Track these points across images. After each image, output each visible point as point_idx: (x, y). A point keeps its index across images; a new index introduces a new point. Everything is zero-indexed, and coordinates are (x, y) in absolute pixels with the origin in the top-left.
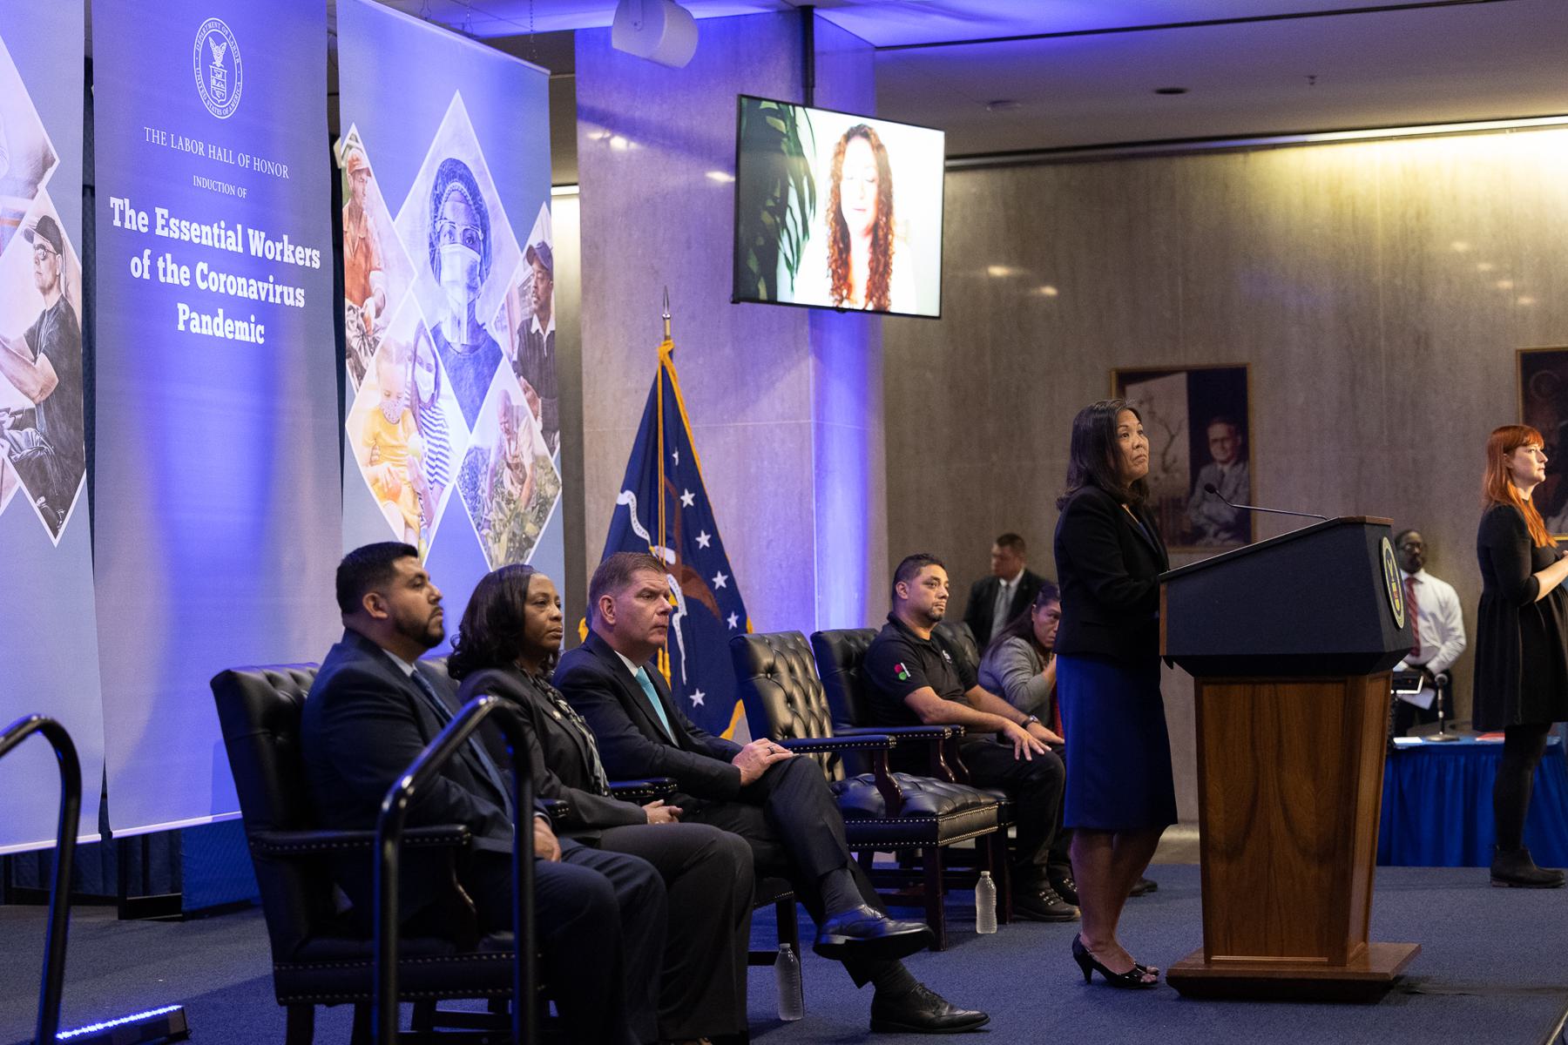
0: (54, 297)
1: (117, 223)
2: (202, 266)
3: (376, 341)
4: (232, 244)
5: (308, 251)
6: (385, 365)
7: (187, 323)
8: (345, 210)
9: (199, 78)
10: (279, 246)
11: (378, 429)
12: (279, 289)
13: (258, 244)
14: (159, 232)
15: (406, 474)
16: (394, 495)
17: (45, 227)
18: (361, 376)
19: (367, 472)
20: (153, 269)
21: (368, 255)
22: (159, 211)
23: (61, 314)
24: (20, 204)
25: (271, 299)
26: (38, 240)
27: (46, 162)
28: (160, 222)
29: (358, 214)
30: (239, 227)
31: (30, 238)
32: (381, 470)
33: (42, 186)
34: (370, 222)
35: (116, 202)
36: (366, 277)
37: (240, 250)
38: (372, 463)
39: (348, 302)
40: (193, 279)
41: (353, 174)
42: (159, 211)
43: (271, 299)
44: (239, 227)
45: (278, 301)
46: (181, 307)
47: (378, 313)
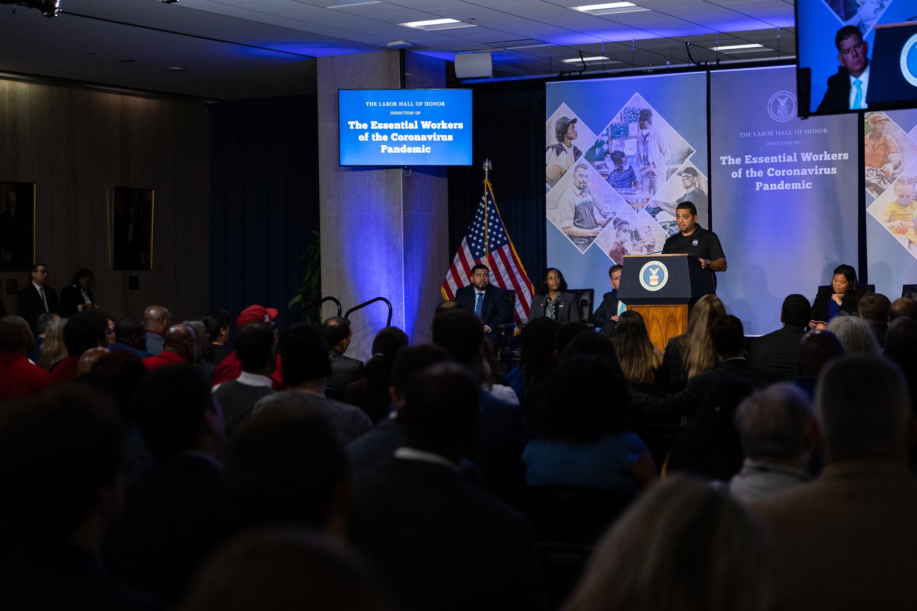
0: (692, 189)
1: (724, 163)
2: (769, 170)
3: (894, 179)
4: (790, 159)
5: (840, 155)
6: (900, 186)
7: (761, 188)
8: (867, 136)
9: (771, 113)
10: (821, 156)
11: (894, 209)
12: (821, 170)
13: (806, 157)
14: (747, 162)
15: (912, 224)
16: (903, 231)
17: (688, 170)
18: (880, 191)
19: (886, 226)
20: (744, 174)
21: (886, 147)
22: (746, 157)
23: (697, 193)
24: (675, 166)
25: (816, 173)
26: (684, 174)
27: (689, 152)
28: (747, 159)
29: (877, 135)
30: (795, 154)
31: (680, 174)
32: (896, 223)
33: (687, 160)
34: (888, 137)
35: (723, 158)
36: (885, 156)
37: (795, 160)
38: (890, 221)
39: (867, 168)
40: (765, 174)
41: (875, 123)
42: (746, 157)
43: (816, 173)
44: (795, 154)
45: (821, 173)
46: (757, 183)
47: (895, 168)
